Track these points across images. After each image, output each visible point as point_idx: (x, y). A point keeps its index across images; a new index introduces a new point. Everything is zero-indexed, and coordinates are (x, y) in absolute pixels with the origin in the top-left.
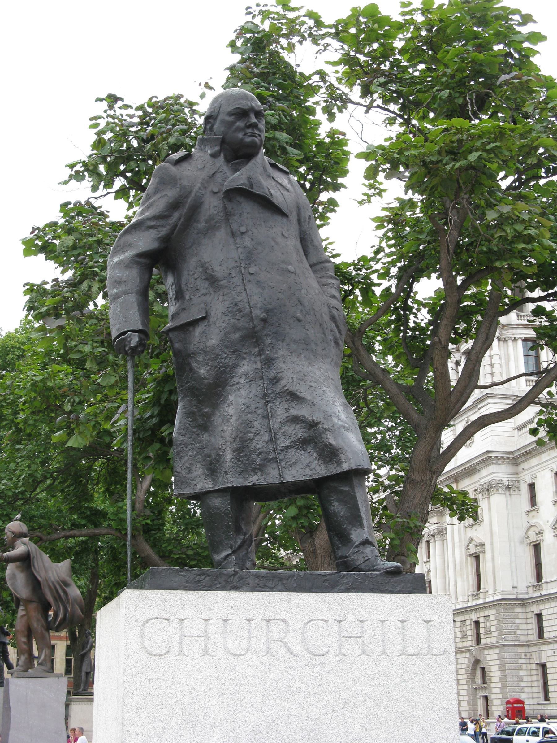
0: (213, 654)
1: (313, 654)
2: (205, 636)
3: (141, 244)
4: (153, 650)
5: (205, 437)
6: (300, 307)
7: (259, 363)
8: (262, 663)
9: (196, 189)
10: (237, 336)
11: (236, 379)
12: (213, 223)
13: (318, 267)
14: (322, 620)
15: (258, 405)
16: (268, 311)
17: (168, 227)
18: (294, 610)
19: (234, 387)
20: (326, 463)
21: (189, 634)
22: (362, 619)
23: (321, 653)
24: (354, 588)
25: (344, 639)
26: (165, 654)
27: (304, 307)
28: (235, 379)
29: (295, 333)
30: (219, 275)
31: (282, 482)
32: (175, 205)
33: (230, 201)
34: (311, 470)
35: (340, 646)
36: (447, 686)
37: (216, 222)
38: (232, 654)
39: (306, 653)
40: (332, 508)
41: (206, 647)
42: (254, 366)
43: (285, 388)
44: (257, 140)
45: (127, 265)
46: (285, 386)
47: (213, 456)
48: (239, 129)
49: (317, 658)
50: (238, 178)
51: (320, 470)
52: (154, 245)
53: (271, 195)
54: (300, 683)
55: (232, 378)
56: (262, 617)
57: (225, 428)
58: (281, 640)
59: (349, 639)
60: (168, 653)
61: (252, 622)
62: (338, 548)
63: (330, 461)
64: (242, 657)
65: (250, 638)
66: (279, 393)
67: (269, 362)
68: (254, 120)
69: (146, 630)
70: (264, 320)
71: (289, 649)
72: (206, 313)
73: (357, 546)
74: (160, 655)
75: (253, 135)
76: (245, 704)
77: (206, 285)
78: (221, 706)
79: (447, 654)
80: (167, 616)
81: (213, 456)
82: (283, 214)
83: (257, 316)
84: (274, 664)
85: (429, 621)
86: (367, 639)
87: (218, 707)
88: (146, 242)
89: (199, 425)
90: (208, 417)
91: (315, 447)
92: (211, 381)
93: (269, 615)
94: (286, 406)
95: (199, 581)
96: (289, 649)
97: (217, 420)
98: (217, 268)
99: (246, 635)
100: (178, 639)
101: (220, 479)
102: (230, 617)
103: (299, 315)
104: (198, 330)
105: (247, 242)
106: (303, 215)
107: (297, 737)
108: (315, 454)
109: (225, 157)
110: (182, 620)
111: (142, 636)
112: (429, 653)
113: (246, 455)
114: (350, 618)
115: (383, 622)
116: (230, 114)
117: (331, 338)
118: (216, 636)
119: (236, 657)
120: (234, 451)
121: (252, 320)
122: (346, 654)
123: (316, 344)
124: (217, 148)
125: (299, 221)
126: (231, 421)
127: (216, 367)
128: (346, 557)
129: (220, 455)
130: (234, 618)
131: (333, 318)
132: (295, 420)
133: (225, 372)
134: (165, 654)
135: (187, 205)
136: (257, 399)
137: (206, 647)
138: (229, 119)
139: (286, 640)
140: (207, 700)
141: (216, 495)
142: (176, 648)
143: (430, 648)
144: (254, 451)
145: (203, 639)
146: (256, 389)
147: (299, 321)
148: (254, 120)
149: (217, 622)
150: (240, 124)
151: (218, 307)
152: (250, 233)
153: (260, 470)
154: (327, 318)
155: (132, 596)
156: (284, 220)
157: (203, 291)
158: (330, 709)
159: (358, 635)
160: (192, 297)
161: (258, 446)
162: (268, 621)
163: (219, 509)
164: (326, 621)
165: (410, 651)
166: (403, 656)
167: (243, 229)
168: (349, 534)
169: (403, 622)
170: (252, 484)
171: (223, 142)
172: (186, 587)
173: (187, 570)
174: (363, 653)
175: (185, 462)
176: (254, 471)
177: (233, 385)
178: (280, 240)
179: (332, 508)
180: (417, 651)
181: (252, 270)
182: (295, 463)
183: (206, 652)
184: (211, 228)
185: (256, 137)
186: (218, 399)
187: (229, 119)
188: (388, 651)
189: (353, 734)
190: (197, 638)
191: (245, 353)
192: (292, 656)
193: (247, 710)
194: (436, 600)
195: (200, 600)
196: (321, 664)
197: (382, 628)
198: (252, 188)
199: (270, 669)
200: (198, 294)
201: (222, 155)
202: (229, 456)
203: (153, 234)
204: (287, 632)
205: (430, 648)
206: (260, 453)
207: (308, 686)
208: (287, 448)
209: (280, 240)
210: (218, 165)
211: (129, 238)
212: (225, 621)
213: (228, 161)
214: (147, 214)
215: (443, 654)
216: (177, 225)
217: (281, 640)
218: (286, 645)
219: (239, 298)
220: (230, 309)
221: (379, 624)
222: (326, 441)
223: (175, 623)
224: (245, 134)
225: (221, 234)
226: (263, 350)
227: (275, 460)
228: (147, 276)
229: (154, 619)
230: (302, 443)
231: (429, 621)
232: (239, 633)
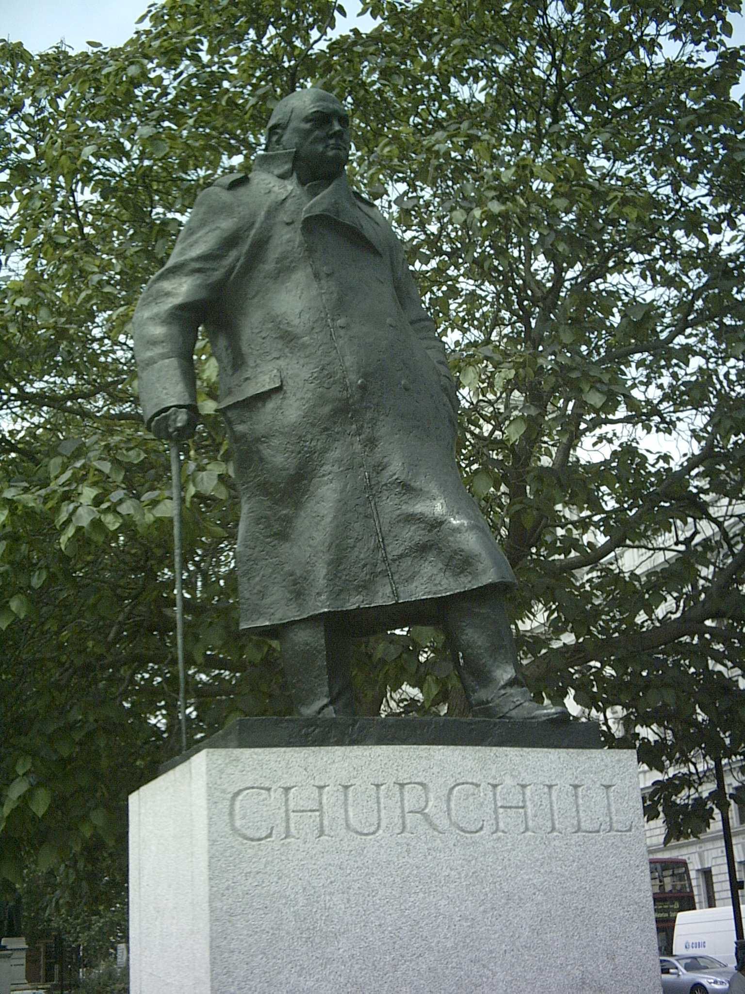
0: (332, 834)
1: (463, 831)
2: (320, 809)
4: (250, 833)
5: (285, 547)
8: (398, 844)
10: (327, 409)
11: (327, 468)
12: (287, 262)
14: (472, 784)
15: (358, 501)
17: (223, 270)
18: (435, 770)
19: (326, 478)
21: (299, 808)
22: (524, 783)
23: (473, 829)
25: (501, 810)
26: (266, 837)
28: (325, 468)
30: (298, 331)
31: (397, 603)
32: (231, 241)
34: (436, 585)
35: (497, 819)
37: (292, 262)
38: (357, 832)
40: (464, 637)
43: (395, 477)
46: (395, 474)
47: (298, 573)
48: (317, 140)
49: (468, 835)
51: (449, 585)
54: (448, 870)
55: (322, 466)
56: (394, 780)
57: (315, 535)
58: (421, 812)
60: (270, 835)
61: (383, 787)
62: (474, 691)
63: (461, 572)
66: (386, 485)
67: (371, 443)
70: (363, 388)
71: (431, 824)
72: (282, 381)
73: (504, 687)
74: (260, 839)
76: (378, 902)
77: (280, 346)
78: (348, 905)
81: (298, 573)
82: (376, 253)
84: (413, 844)
87: (343, 906)
89: (275, 534)
90: (288, 521)
92: (292, 472)
93: (403, 777)
94: (397, 501)
95: (307, 735)
96: (431, 824)
98: (296, 322)
100: (284, 815)
101: (310, 604)
102: (352, 782)
104: (271, 405)
107: (449, 945)
108: (440, 565)
109: (299, 178)
113: (344, 569)
114: (508, 781)
116: (307, 120)
118: (335, 809)
119: (363, 837)
120: (329, 565)
122: (506, 830)
124: (287, 167)
126: (323, 523)
127: (299, 452)
128: (488, 702)
129: (308, 572)
130: (357, 782)
132: (411, 519)
134: (266, 837)
135: (249, 241)
140: (328, 898)
141: (303, 626)
142: (282, 829)
145: (317, 813)
148: (337, 127)
149: (335, 789)
153: (365, 587)
155: (215, 757)
157: (275, 354)
159: (521, 804)
160: (258, 362)
161: (362, 556)
162: (402, 786)
163: (307, 644)
164: (478, 786)
168: (490, 672)
170: (354, 607)
171: (296, 158)
172: (290, 743)
173: (290, 720)
175: (257, 584)
177: (324, 475)
179: (464, 637)
183: (322, 833)
184: (284, 270)
186: (303, 495)
189: (522, 940)
190: (309, 814)
191: (338, 433)
192: (436, 833)
193: (381, 909)
196: (474, 843)
198: (338, 216)
199: (408, 851)
200: (269, 358)
201: (295, 175)
202: (321, 571)
206: (365, 566)
207: (459, 873)
208: (401, 556)
210: (290, 188)
212: (346, 787)
213: (302, 182)
216: (234, 267)
217: (421, 812)
218: (426, 817)
220: (315, 375)
223: (277, 795)
227: (384, 573)
230: (422, 550)
232: (365, 803)
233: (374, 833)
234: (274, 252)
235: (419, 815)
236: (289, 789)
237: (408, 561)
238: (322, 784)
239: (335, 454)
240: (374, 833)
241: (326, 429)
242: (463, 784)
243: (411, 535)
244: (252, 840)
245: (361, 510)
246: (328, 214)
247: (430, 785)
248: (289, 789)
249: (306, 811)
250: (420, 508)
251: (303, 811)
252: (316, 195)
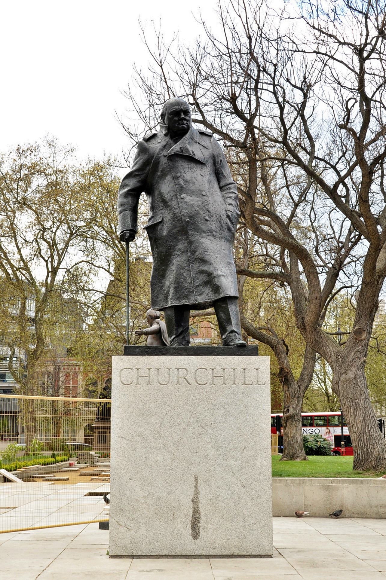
3: (131, 184)
6: (208, 213)
7: (186, 244)
9: (156, 155)
10: (175, 231)
11: (176, 252)
13: (225, 188)
16: (190, 217)
20: (215, 293)
27: (210, 213)
30: (167, 200)
32: (146, 164)
33: (171, 160)
41: (149, 381)
42: (184, 245)
45: (126, 195)
50: (176, 147)
51: (212, 297)
52: (138, 184)
53: (194, 154)
65: (169, 377)
67: (191, 243)
68: (183, 116)
69: (122, 373)
70: (188, 222)
83: (185, 220)
86: (226, 377)
88: (132, 183)
91: (211, 286)
97: (168, 273)
98: (166, 196)
99: (167, 376)
103: (207, 218)
104: (159, 227)
105: (181, 181)
106: (217, 160)
110: (138, 369)
111: (120, 376)
114: (218, 367)
115: (234, 369)
116: (170, 114)
117: (225, 227)
121: (182, 222)
123: (216, 232)
125: (215, 163)
131: (228, 216)
132: (202, 272)
133: (170, 249)
136: (185, 262)
137: (149, 381)
138: (171, 116)
142: (135, 381)
143: (258, 381)
144: (184, 288)
146: (184, 258)
147: (207, 220)
150: (176, 119)
151: (167, 215)
153: (186, 297)
154: (224, 217)
157: (161, 208)
158: (206, 409)
162: (178, 369)
167: (179, 174)
169: (244, 369)
174: (224, 383)
176: (184, 298)
178: (199, 178)
180: (251, 383)
181: (182, 196)
182: (202, 293)
184: (164, 175)
187: (171, 116)
188: (236, 383)
195: (146, 360)
202: (172, 291)
203: (138, 178)
204: (188, 374)
205: (258, 381)
208: (199, 286)
209: (199, 178)
210: (167, 140)
211: (127, 181)
212: (158, 369)
213: (172, 138)
214: (134, 168)
219: (176, 211)
221: (232, 370)
222: (215, 283)
223: (135, 370)
224: (179, 124)
225: (169, 178)
226: (188, 237)
228: (135, 201)
234: (160, 169)
237: (201, 288)
239: (178, 247)
243: (203, 278)
245: (186, 268)
247: (188, 369)
250: (205, 268)
252: (177, 143)
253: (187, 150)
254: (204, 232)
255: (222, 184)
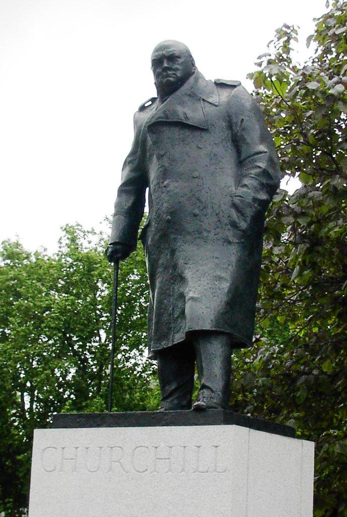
0: (78, 470)
4: (49, 469)
18: (127, 440)
24: (171, 423)
25: (157, 460)
26: (53, 471)
29: (190, 227)
36: (225, 496)
39: (133, 470)
44: (171, 79)
53: (187, 118)
56: (107, 445)
59: (161, 460)
61: (102, 449)
64: (94, 473)
67: (173, 252)
70: (168, 221)
75: (168, 76)
79: (227, 471)
80: (55, 446)
85: (217, 447)
103: (197, 211)
106: (234, 120)
110: (63, 448)
112: (215, 470)
114: (162, 445)
115: (185, 447)
119: (92, 473)
125: (230, 126)
131: (234, 205)
139: (121, 461)
145: (73, 460)
147: (195, 215)
152: (168, 153)
156: (203, 134)
159: (167, 457)
165: (201, 469)
166: (196, 473)
174: (170, 470)
180: (206, 469)
185: (170, 77)
190: (70, 460)
194: (223, 430)
197: (184, 453)
199: (110, 481)
212: (87, 448)
215: (225, 471)
221: (182, 449)
229: (48, 448)
231: (217, 447)
233: (96, 471)
235: (118, 463)
236: (64, 448)
238: (76, 447)
239: (161, 262)
240: (96, 471)
241: (158, 247)
242: (140, 447)
244: (48, 472)
246: (160, 120)
248: (64, 448)
249: (68, 459)
251: (68, 459)
253: (175, 112)
254: (189, 233)
255: (243, 156)
